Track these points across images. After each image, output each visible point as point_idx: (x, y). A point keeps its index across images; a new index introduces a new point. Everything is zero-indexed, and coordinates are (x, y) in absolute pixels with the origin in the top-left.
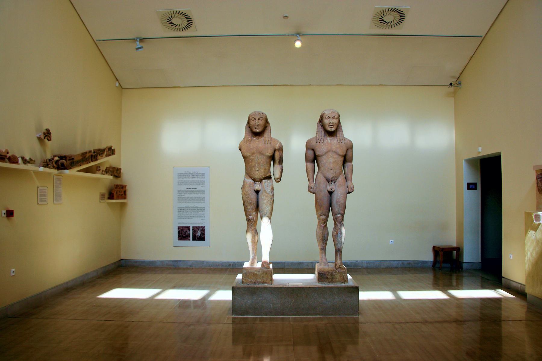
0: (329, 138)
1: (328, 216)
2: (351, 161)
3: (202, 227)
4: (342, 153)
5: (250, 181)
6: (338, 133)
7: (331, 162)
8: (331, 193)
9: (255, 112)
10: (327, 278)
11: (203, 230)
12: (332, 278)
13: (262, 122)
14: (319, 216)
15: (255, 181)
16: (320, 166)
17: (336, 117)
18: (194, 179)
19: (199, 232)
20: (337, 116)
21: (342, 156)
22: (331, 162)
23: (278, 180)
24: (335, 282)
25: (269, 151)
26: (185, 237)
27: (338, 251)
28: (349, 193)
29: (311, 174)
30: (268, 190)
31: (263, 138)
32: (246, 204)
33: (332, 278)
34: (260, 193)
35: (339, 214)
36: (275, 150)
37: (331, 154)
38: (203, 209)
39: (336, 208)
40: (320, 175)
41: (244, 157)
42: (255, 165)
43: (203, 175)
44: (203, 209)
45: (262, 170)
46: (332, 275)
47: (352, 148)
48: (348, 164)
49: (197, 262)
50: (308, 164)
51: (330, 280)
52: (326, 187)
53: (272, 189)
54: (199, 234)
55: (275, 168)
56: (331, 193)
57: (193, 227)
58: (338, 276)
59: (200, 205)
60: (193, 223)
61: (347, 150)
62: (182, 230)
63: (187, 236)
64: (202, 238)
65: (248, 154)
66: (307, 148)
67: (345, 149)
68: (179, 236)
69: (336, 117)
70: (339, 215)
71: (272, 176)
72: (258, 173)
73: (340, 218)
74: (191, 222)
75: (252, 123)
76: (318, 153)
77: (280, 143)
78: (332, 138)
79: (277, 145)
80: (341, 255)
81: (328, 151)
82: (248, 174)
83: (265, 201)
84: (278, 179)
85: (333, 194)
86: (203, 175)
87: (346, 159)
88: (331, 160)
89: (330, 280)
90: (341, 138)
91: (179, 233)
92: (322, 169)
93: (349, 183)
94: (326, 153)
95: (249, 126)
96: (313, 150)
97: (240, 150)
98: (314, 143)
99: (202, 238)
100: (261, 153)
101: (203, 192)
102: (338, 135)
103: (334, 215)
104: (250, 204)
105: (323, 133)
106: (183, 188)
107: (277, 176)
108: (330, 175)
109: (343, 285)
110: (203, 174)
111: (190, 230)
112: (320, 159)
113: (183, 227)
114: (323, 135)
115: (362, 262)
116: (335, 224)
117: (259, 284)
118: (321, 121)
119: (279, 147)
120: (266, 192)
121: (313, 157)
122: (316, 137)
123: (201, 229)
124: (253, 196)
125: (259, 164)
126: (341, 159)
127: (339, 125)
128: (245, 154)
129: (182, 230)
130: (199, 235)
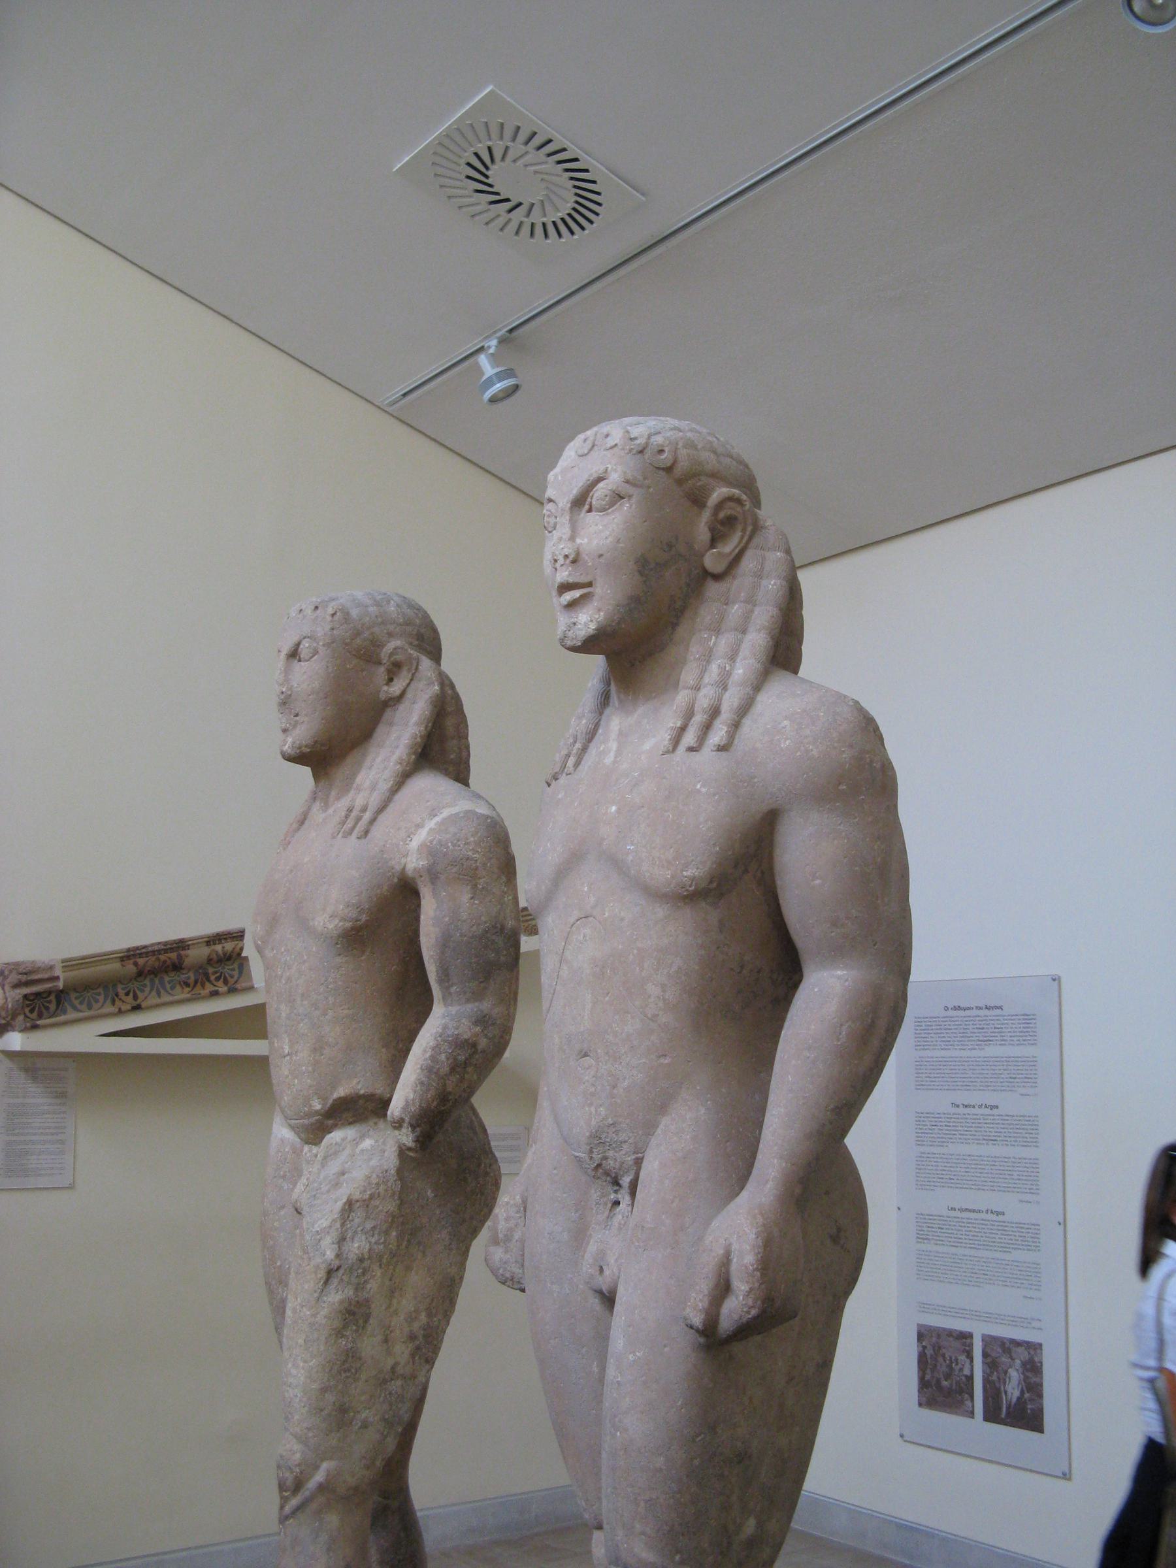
18: (992, 1051)
19: (1014, 1375)
26: (949, 1393)
37: (589, 884)
38: (1029, 1236)
43: (1027, 1026)
52: (580, 1235)
54: (1013, 1389)
57: (988, 1341)
62: (937, 1348)
64: (1026, 1415)
68: (923, 1384)
99: (1026, 1415)
101: (1025, 1130)
110: (1028, 1020)
111: (970, 1357)
123: (1022, 1354)
129: (937, 1348)
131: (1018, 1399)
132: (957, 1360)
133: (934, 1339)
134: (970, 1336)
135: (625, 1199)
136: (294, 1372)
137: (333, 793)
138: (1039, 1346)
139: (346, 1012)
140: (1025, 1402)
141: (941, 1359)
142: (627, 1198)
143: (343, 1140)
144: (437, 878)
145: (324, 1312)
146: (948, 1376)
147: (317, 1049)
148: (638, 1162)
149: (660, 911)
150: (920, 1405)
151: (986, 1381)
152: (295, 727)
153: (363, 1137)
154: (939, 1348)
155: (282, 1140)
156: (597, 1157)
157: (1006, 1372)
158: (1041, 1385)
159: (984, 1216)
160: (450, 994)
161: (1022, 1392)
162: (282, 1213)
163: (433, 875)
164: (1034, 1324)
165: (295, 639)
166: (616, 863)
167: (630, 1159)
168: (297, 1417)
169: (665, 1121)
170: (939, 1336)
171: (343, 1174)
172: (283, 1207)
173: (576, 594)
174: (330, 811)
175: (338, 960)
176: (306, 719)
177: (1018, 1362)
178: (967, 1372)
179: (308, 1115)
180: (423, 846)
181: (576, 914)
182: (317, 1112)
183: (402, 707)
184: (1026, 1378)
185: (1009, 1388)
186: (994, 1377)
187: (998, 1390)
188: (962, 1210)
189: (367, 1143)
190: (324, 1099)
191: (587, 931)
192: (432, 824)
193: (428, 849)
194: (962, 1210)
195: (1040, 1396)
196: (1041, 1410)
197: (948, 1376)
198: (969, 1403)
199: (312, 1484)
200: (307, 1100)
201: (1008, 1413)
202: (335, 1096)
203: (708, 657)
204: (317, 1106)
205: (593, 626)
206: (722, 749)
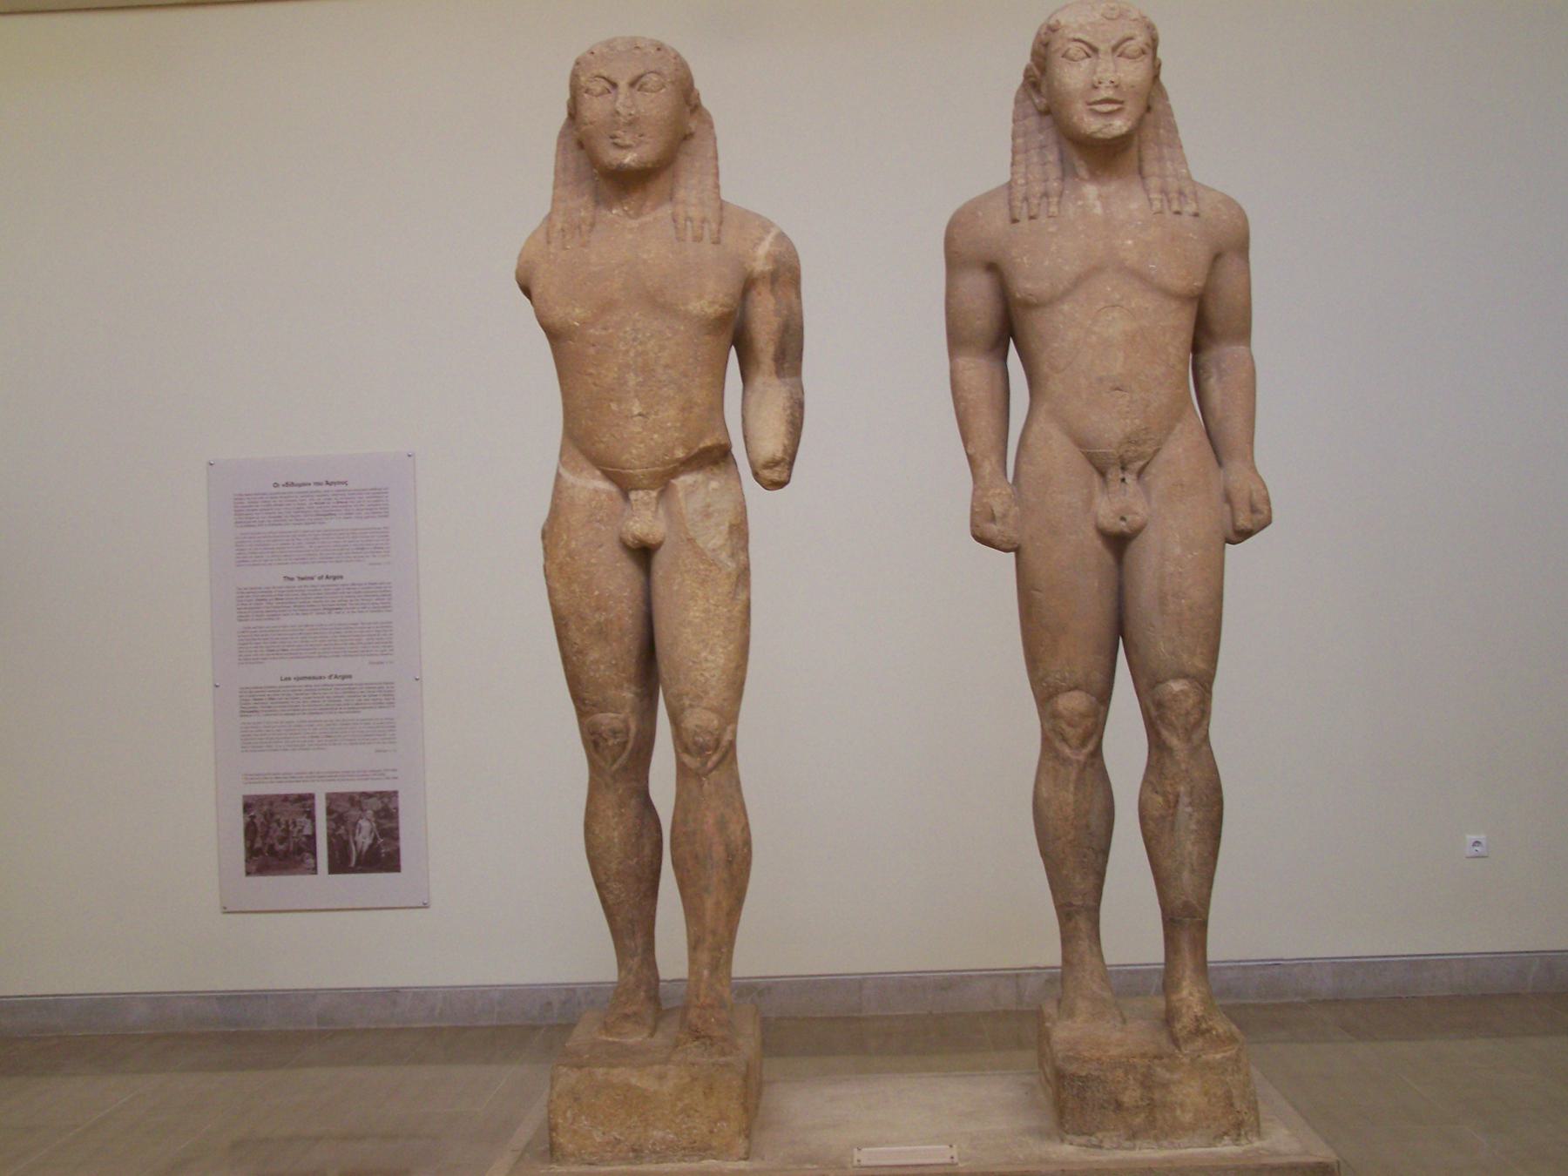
0: (1091, 190)
1: (1104, 697)
2: (1244, 334)
3: (381, 795)
4: (1183, 275)
5: (592, 484)
6: (1150, 153)
7: (1109, 339)
8: (1118, 543)
9: (609, 44)
10: (1119, 1106)
11: (386, 810)
12: (1152, 1106)
13: (655, 105)
14: (1045, 696)
15: (624, 484)
16: (1045, 369)
17: (1132, 47)
19: (365, 825)
20: (1141, 39)
21: (1183, 298)
22: (1109, 339)
23: (774, 475)
24: (1174, 1130)
26: (286, 854)
27: (1184, 920)
28: (1243, 535)
29: (984, 422)
30: (714, 539)
31: (666, 211)
32: (574, 635)
33: (1152, 1106)
34: (661, 560)
35: (1182, 675)
36: (748, 284)
38: (383, 694)
39: (1164, 640)
40: (1043, 425)
41: (555, 335)
43: (376, 502)
44: (383, 694)
45: (669, 414)
46: (1147, 1082)
47: (1242, 248)
48: (1224, 354)
49: (359, 996)
50: (962, 361)
51: (1139, 1120)
52: (1089, 501)
53: (739, 531)
54: (364, 837)
55: (753, 399)
56: (1118, 543)
57: (332, 799)
58: (1189, 1093)
59: (362, 670)
60: (332, 776)
61: (1217, 257)
62: (270, 816)
63: (300, 851)
64: (383, 858)
65: (575, 314)
66: (955, 261)
67: (1201, 254)
68: (252, 852)
69: (1132, 47)
70: (1177, 686)
71: (738, 450)
72: (646, 432)
73: (1191, 702)
74: (320, 770)
75: (595, 108)
76: (1024, 286)
77: (781, 237)
78: (1113, 187)
79: (764, 249)
80: (1200, 944)
81: (1096, 270)
82: (581, 440)
83: (695, 613)
84: (773, 464)
85: (1134, 548)
86: (376, 502)
87: (1211, 323)
88: (1116, 326)
89: (1139, 1120)
90: (1173, 184)
91: (250, 830)
92: (1055, 386)
93: (1236, 474)
94: (1079, 281)
95: (579, 138)
96: (992, 268)
97: (527, 291)
98: (996, 221)
99: (383, 858)
100: (657, 302)
101: (379, 596)
102: (1151, 167)
103: (1147, 685)
104: (601, 633)
105: (1052, 157)
106: (270, 576)
107: (771, 444)
108: (1111, 426)
109: (1227, 1149)
111: (311, 816)
112: (1038, 324)
113: (270, 800)
114: (1054, 172)
115: (1308, 964)
116: (1157, 745)
117: (661, 1157)
118: (1039, 78)
119: (774, 258)
120: (700, 554)
121: (999, 321)
122: (1009, 186)
123: (376, 804)
124: (619, 579)
126: (1180, 321)
127: (1151, 99)
128: (558, 314)
129: (270, 816)
130: (365, 838)
131: (371, 846)
132: (295, 823)
133: (265, 808)
134: (311, 797)
135: (1130, 478)
136: (711, 657)
137: (649, 204)
138: (395, 793)
140: (379, 848)
141: (274, 825)
142: (1134, 476)
145: (739, 608)
146: (282, 840)
147: (687, 408)
148: (1156, 452)
149: (1174, 305)
150: (248, 873)
151: (331, 835)
152: (638, 145)
153: (709, 479)
154: (272, 815)
155: (596, 491)
156: (1122, 451)
157: (355, 824)
158: (397, 828)
159: (327, 681)
161: (375, 839)
163: (774, 278)
164: (390, 774)
166: (1140, 276)
167: (1150, 450)
168: (712, 694)
169: (1179, 426)
170: (271, 804)
171: (709, 506)
173: (1115, 107)
174: (648, 218)
177: (370, 812)
178: (307, 831)
179: (664, 463)
181: (1102, 304)
182: (678, 460)
183: (695, 142)
184: (379, 825)
185: (359, 838)
186: (342, 831)
187: (347, 842)
188: (298, 679)
189: (714, 484)
191: (1116, 314)
192: (769, 238)
193: (768, 255)
194: (298, 679)
195: (397, 839)
196: (398, 851)
197: (282, 840)
198: (311, 861)
199: (725, 742)
201: (358, 862)
202: (702, 445)
203: (1160, 159)
204: (680, 454)
205: (1125, 129)
206: (1196, 215)
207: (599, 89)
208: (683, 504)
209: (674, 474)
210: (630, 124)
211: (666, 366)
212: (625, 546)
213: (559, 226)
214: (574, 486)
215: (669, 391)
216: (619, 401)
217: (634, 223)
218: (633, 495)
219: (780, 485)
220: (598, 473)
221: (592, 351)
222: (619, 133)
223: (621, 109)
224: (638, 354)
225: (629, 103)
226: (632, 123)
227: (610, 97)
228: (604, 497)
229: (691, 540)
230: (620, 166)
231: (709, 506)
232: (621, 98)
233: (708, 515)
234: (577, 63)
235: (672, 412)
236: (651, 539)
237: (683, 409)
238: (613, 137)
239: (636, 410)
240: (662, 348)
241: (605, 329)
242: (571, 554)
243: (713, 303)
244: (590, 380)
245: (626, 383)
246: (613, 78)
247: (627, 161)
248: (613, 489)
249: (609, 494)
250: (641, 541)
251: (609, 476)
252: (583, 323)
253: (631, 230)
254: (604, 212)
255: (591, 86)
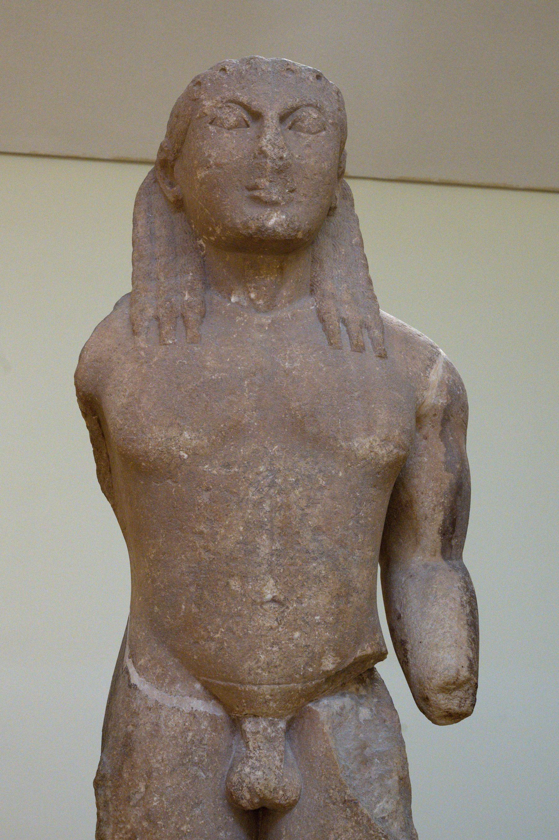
5: (182, 706)
15: (234, 707)
23: (451, 703)
25: (383, 416)
42: (249, 548)
45: (317, 601)
75: (225, 146)
84: (451, 687)
100: (306, 432)
125: (287, 532)
139: (370, 554)
143: (342, 708)
144: (449, 420)
152: (289, 202)
155: (193, 714)
160: (451, 547)
162: (197, 811)
165: (290, 103)
171: (364, 747)
172: (198, 804)
174: (285, 313)
175: (372, 491)
176: (303, 199)
179: (305, 678)
180: (441, 383)
190: (343, 657)
200: (316, 658)
202: (359, 654)
204: (329, 664)
207: (232, 120)
208: (332, 743)
209: (313, 695)
210: (280, 171)
211: (317, 530)
212: (232, 802)
213: (150, 312)
214: (158, 707)
215: (318, 567)
216: (244, 577)
217: (266, 319)
218: (249, 726)
219: (454, 717)
220: (198, 686)
221: (205, 497)
222: (264, 182)
223: (268, 149)
224: (275, 508)
225: (280, 141)
226: (282, 171)
227: (250, 132)
228: (205, 724)
229: (351, 804)
230: (261, 230)
231: (364, 747)
232: (269, 135)
233: (366, 762)
234: (197, 83)
235: (323, 600)
236: (280, 798)
237: (339, 596)
238: (255, 188)
239: (269, 597)
240: (312, 502)
241: (228, 466)
242: (148, 816)
243: (386, 440)
244: (200, 543)
245: (254, 551)
246: (255, 105)
247: (271, 223)
248: (220, 713)
249: (213, 718)
250: (263, 799)
251: (212, 693)
252: (194, 453)
253: (262, 326)
254: (217, 298)
255: (219, 113)
